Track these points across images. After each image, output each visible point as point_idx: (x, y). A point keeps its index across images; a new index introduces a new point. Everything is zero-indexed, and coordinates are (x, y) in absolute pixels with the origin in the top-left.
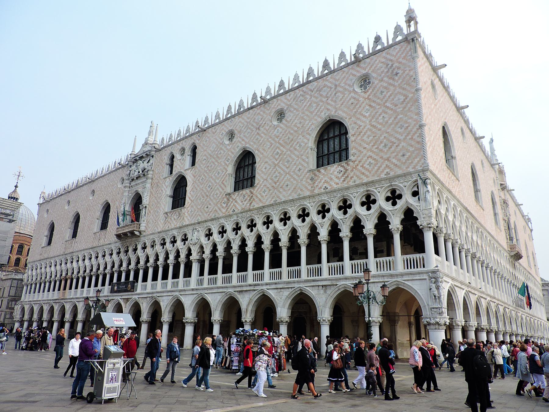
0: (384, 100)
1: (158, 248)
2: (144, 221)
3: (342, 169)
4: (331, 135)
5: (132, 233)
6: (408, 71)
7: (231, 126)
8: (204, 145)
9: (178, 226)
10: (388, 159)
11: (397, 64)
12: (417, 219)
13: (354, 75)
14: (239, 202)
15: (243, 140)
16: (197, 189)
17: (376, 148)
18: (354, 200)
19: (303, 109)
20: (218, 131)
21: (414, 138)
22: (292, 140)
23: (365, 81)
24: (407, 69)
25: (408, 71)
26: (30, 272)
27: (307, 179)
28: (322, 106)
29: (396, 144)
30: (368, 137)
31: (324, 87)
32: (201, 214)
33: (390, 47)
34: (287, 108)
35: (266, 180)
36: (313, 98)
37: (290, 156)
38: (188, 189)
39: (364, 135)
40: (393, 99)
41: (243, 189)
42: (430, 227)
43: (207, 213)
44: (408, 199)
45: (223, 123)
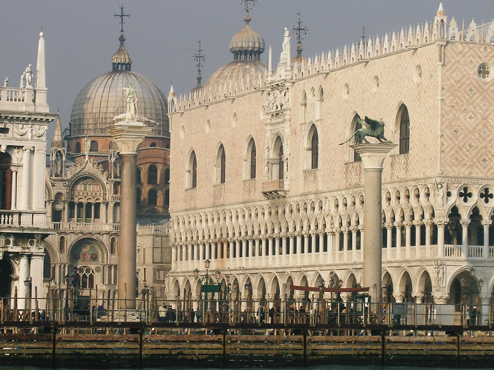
2: (287, 178)
5: (276, 192)
14: (353, 174)
20: (338, 80)
26: (176, 226)
36: (394, 75)
38: (319, 145)
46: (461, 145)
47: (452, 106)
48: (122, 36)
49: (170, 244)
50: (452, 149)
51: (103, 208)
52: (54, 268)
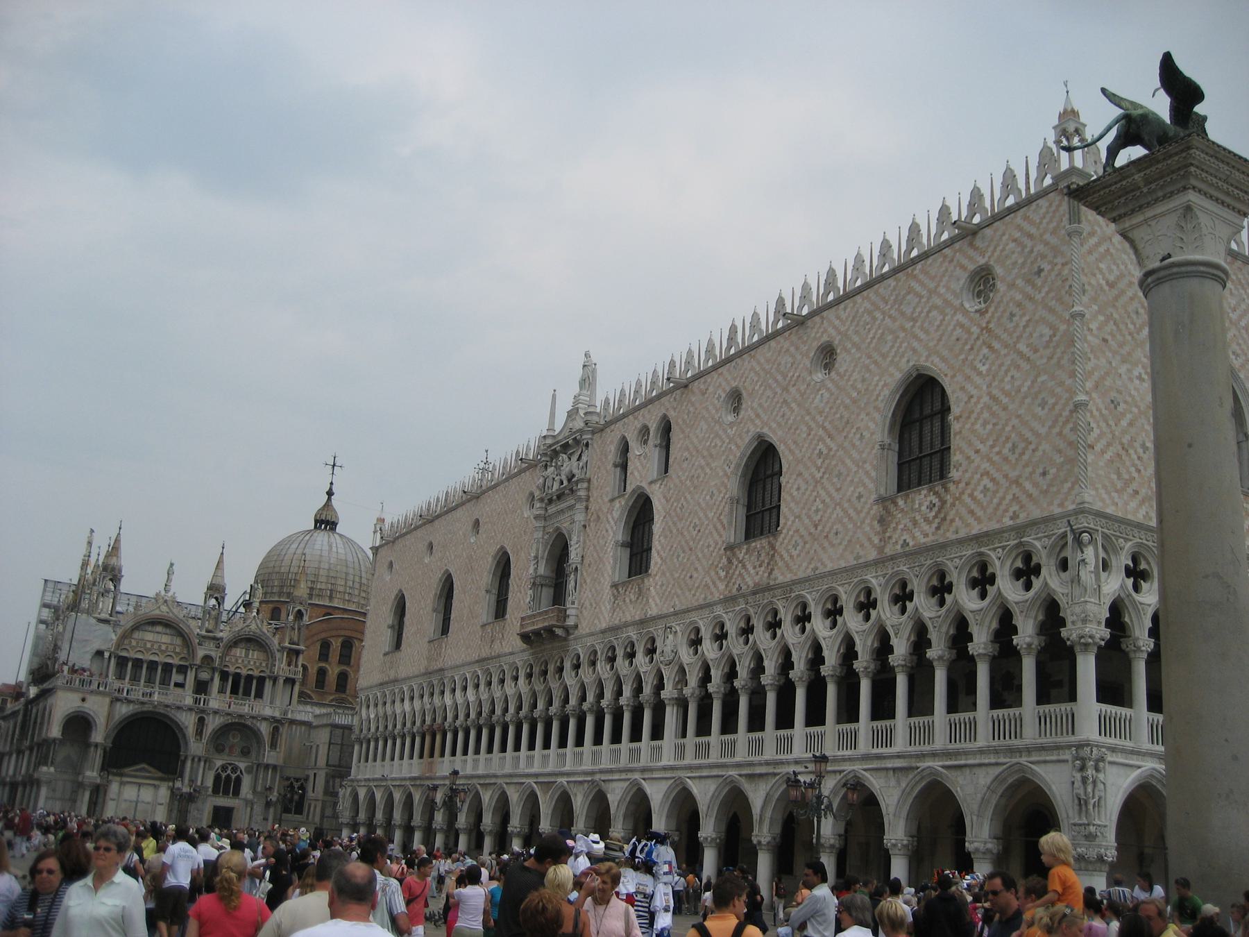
0: (1015, 335)
1: (602, 668)
2: (573, 603)
3: (935, 500)
4: (927, 411)
5: (550, 630)
6: (1059, 267)
7: (734, 379)
8: (684, 420)
9: (637, 618)
10: (1017, 482)
11: (1040, 248)
12: (1062, 623)
13: (963, 267)
15: (758, 416)
17: (998, 453)
18: (955, 574)
20: (711, 389)
21: (1066, 430)
22: (848, 422)
23: (982, 281)
24: (1059, 260)
25: (1059, 267)
28: (902, 343)
29: (1032, 447)
31: (909, 293)
32: (679, 592)
33: (1030, 201)
35: (799, 517)
36: (887, 320)
37: (843, 462)
38: (657, 527)
39: (977, 419)
40: (1031, 334)
41: (762, 534)
42: (1086, 645)
44: (1050, 579)
45: (720, 370)
46: (1125, 441)
47: (1105, 340)
48: (331, 489)
49: (353, 737)
50: (1109, 445)
51: (268, 684)
52: (184, 762)
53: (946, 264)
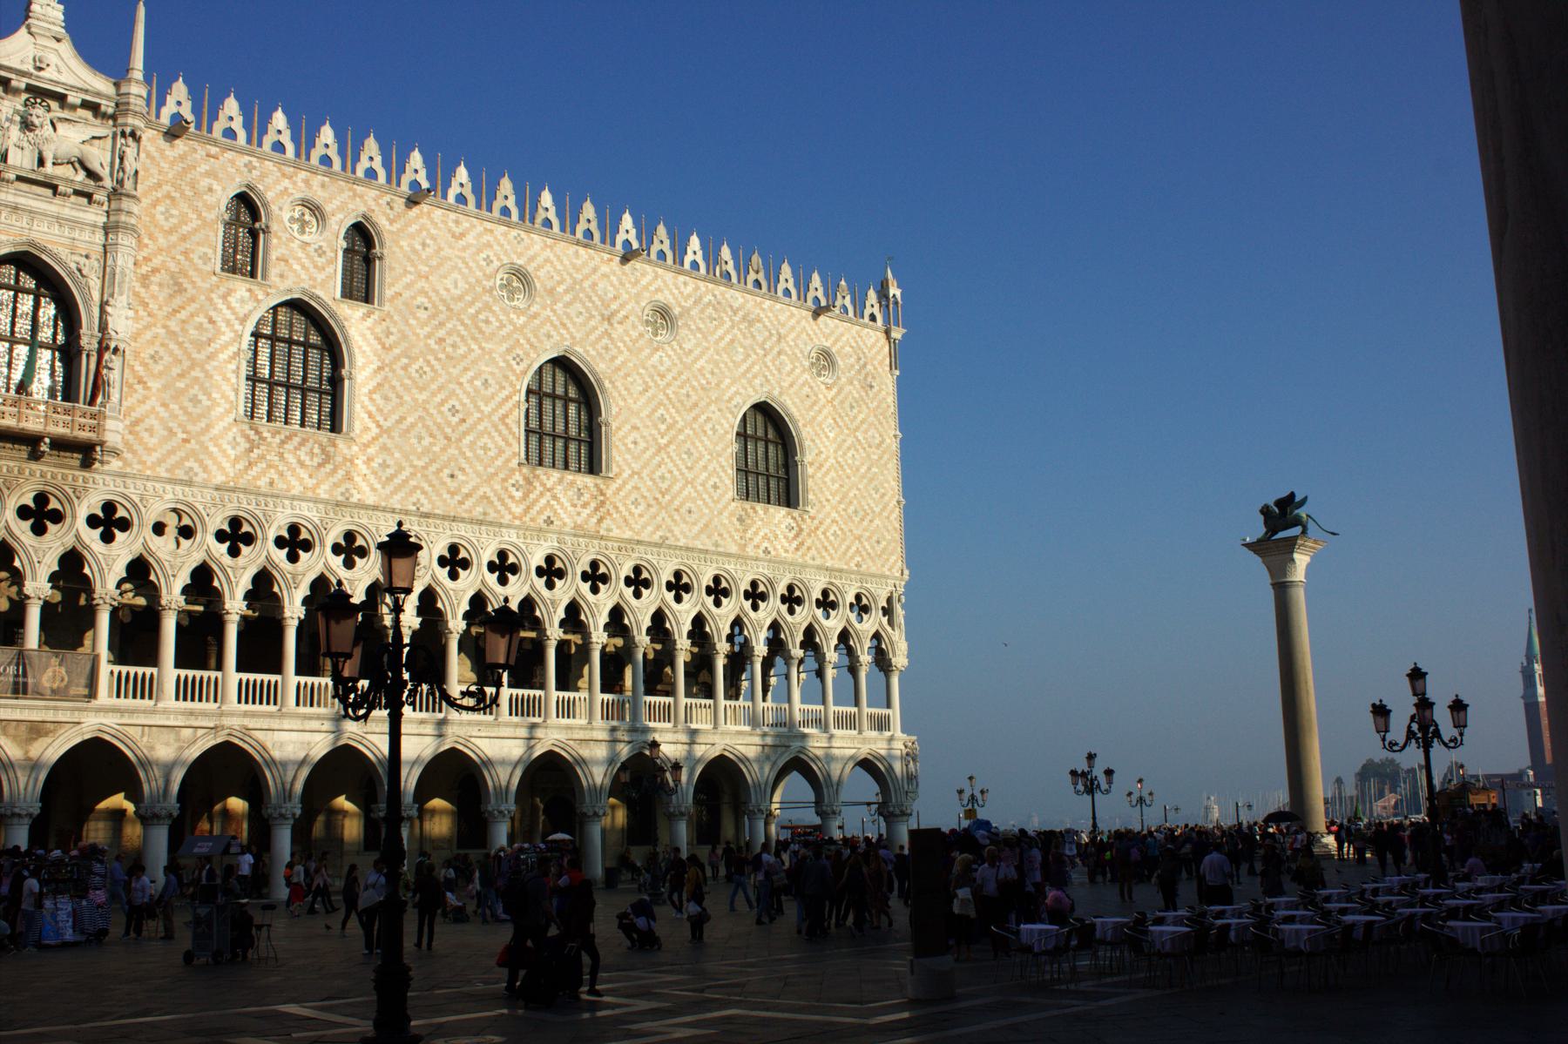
8: (415, 251)
9: (323, 492)
15: (564, 325)
16: (399, 397)
19: (717, 342)
20: (470, 238)
22: (696, 405)
27: (732, 514)
30: (833, 481)
31: (759, 321)
32: (426, 486)
34: (681, 315)
43: (453, 494)
45: (489, 225)
53: (793, 321)
